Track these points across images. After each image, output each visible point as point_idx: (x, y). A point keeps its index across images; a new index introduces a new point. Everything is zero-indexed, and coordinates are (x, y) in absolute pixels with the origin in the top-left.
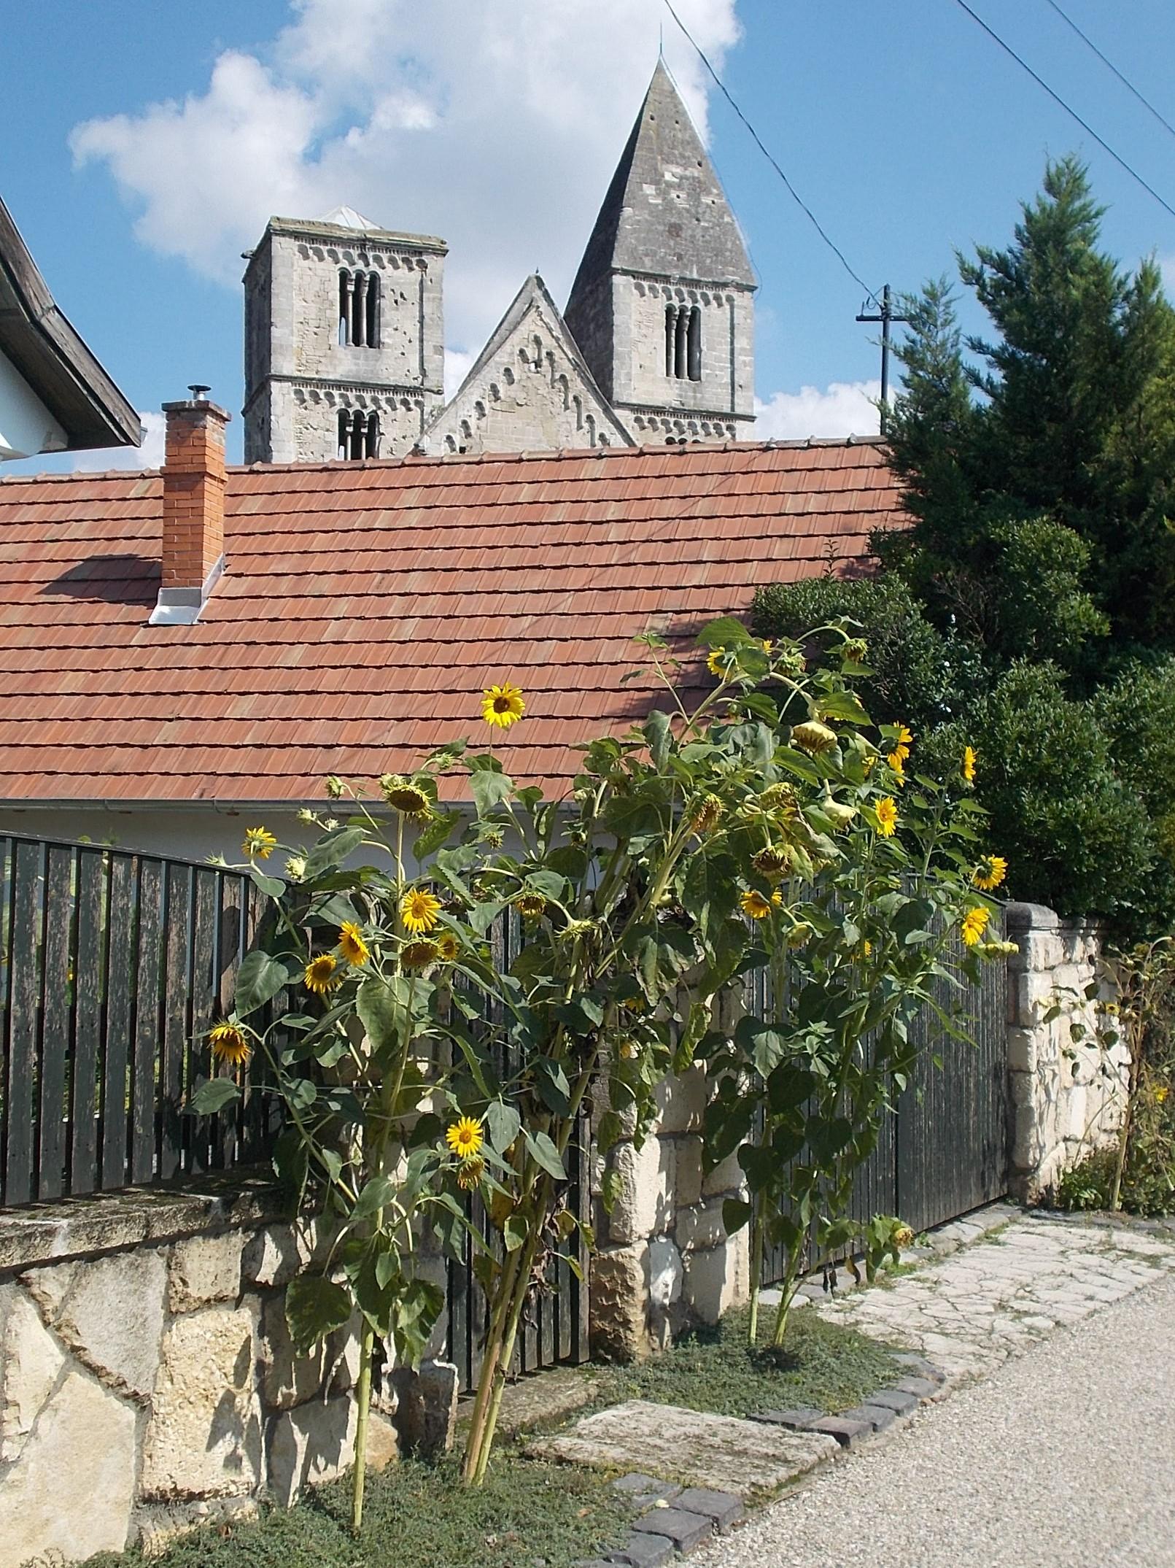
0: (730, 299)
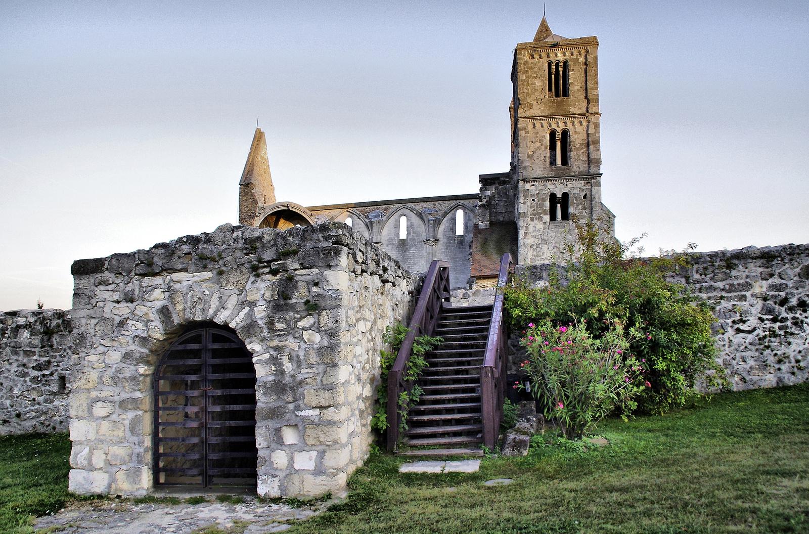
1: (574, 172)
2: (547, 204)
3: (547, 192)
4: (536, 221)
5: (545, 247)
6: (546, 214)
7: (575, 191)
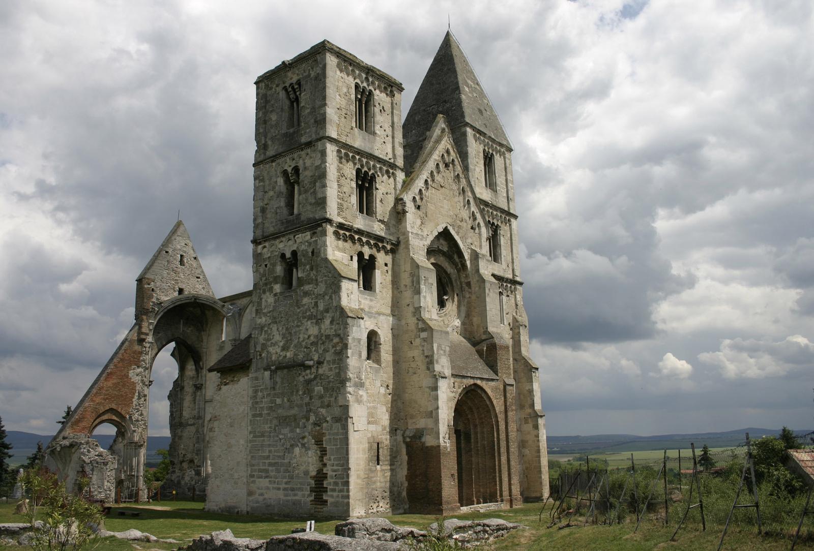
0: (504, 153)
1: (303, 221)
2: (279, 270)
3: (277, 253)
4: (268, 294)
5: (274, 327)
6: (277, 283)
7: (303, 247)
